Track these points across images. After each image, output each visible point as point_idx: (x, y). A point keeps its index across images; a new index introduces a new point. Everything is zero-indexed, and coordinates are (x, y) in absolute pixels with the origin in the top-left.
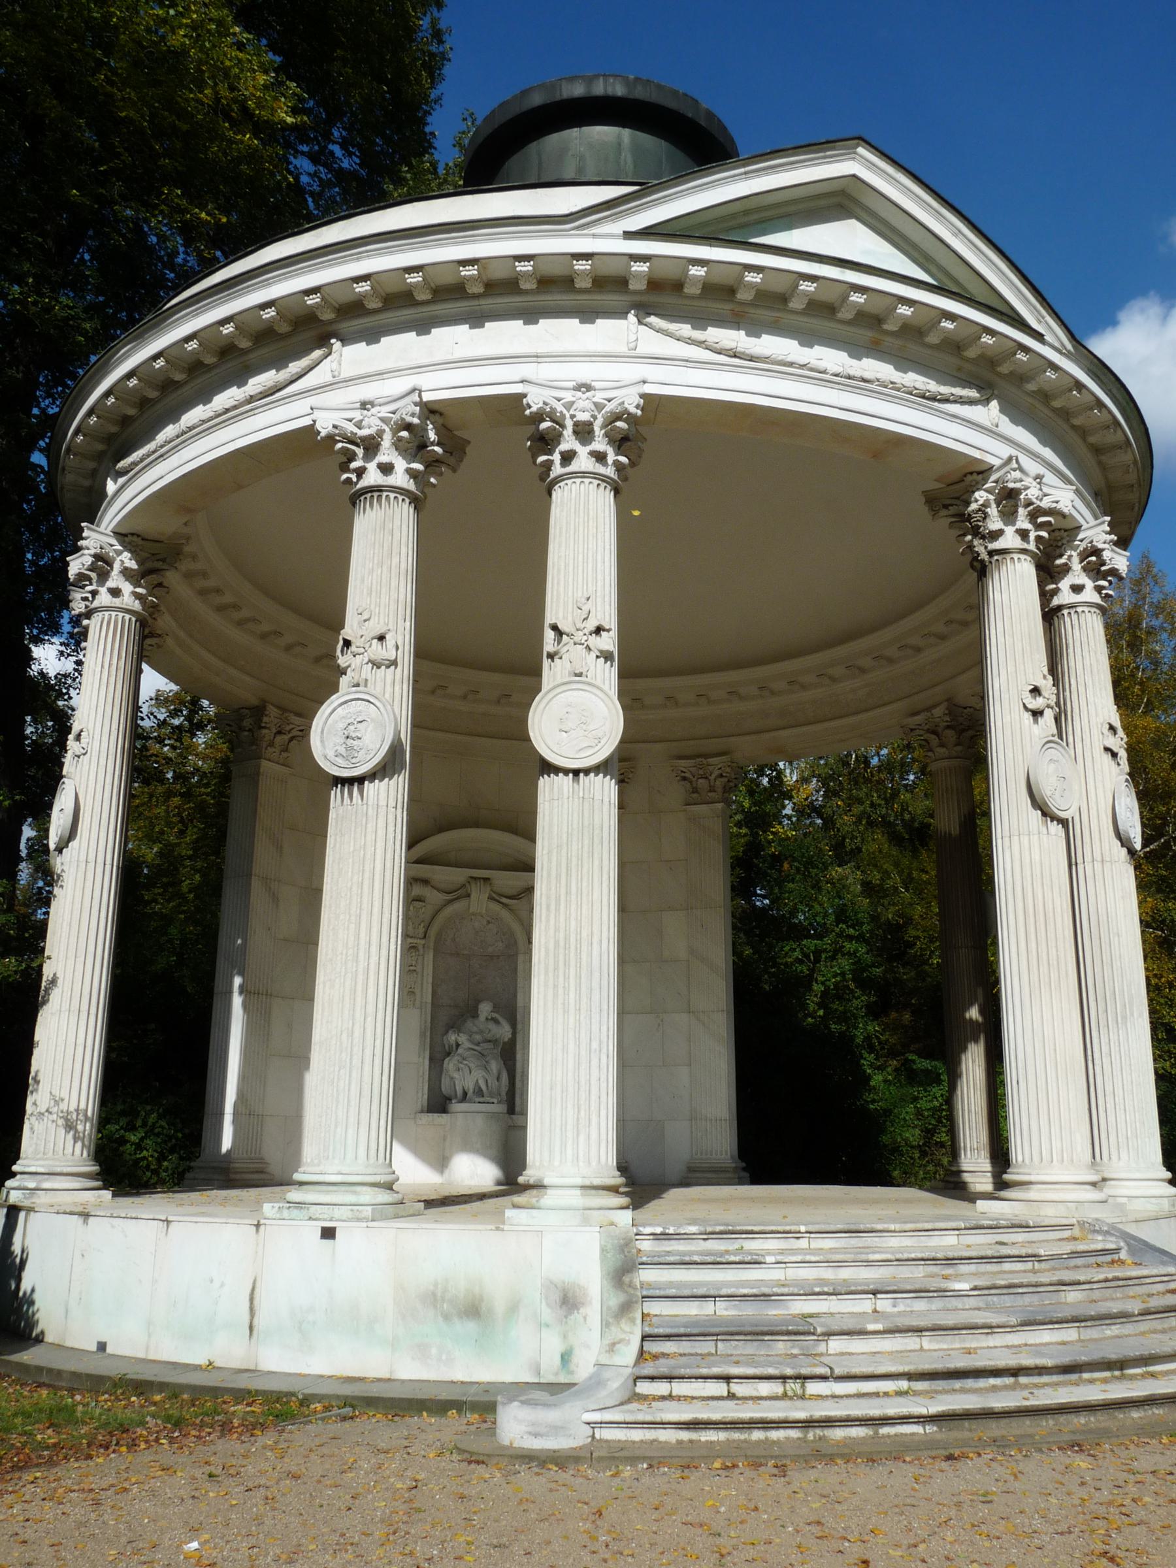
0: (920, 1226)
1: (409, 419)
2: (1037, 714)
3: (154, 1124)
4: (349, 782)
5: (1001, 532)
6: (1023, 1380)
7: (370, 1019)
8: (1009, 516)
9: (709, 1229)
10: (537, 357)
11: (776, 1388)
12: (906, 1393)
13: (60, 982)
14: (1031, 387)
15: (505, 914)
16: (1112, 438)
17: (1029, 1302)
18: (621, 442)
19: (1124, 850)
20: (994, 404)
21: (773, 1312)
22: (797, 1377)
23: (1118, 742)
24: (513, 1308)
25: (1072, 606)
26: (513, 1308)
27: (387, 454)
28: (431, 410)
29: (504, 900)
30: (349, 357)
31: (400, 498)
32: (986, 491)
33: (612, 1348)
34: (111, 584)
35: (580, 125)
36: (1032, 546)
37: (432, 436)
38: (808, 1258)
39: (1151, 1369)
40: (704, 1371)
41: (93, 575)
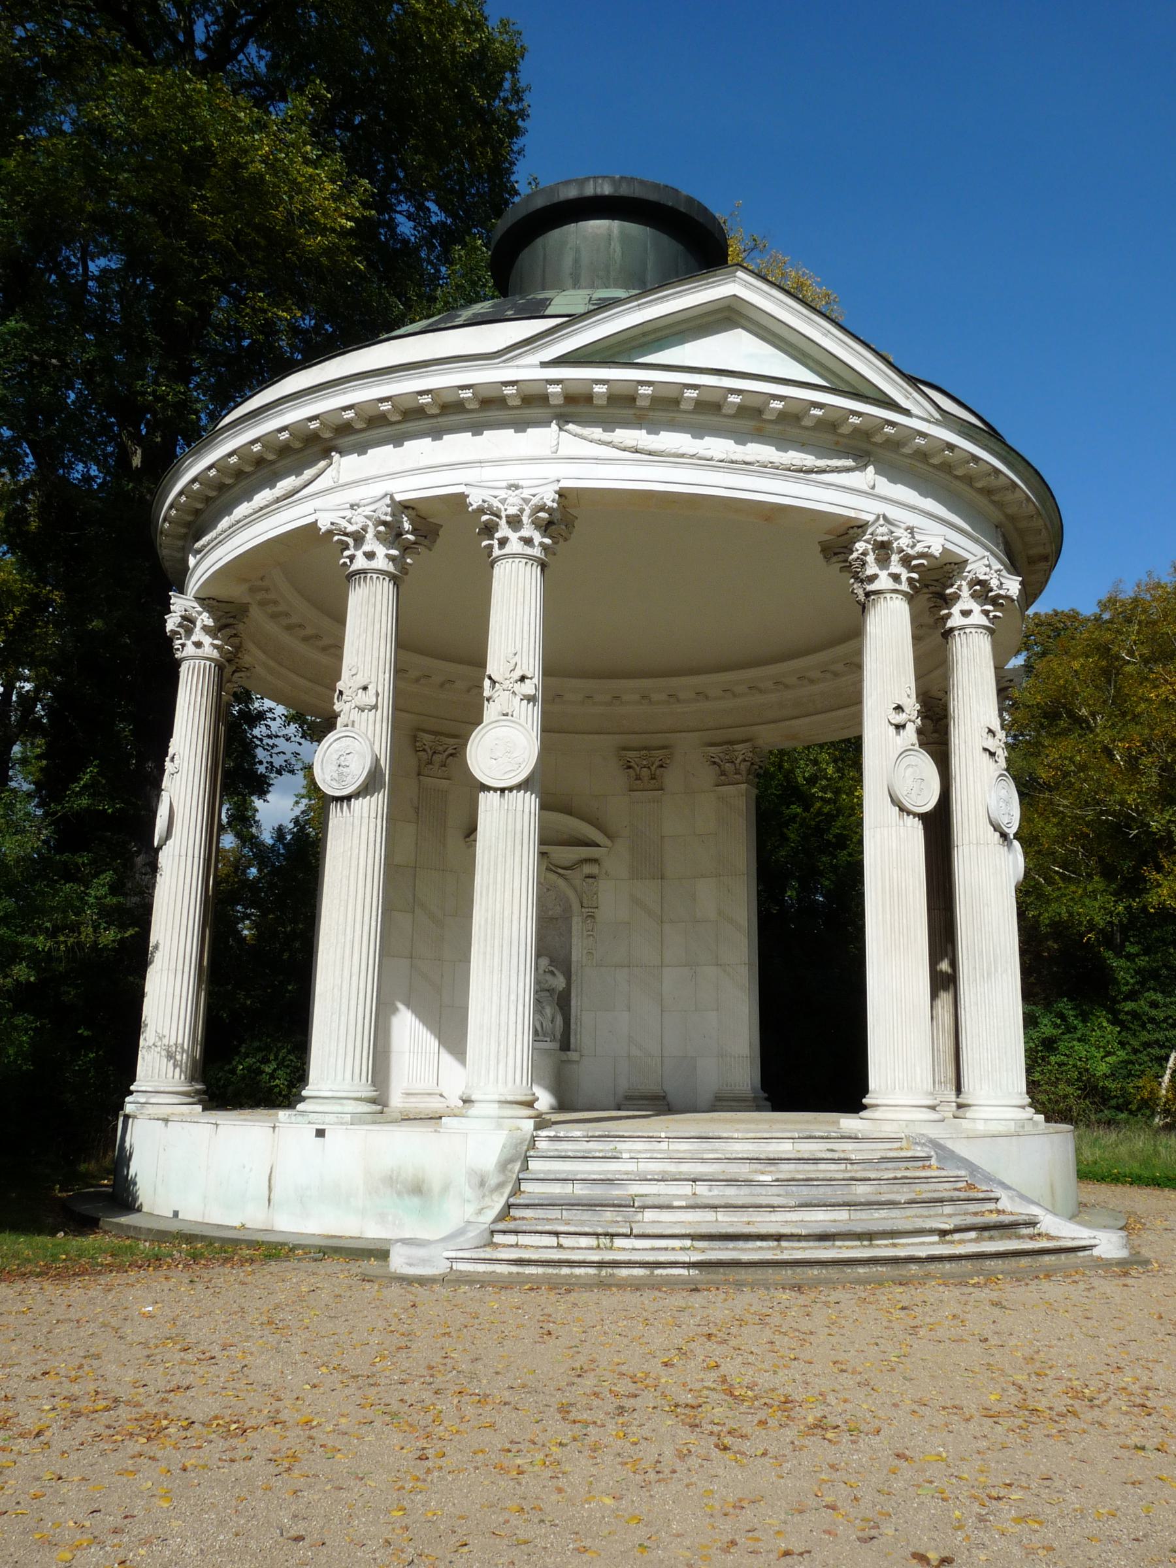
0: (759, 1135)
1: (383, 518)
2: (899, 727)
3: (284, 1058)
4: (340, 799)
5: (875, 577)
6: (784, 1244)
7: (355, 978)
8: (883, 562)
9: (590, 1134)
10: (480, 463)
11: (592, 1242)
12: (689, 1249)
13: (161, 947)
14: (906, 450)
15: (561, 882)
16: (1002, 481)
17: (806, 1193)
18: (546, 527)
19: (997, 834)
20: (871, 469)
21: (616, 1192)
22: (606, 1235)
23: (997, 745)
24: (446, 1188)
25: (961, 628)
26: (446, 1188)
27: (371, 543)
28: (405, 507)
29: (560, 871)
30: (345, 466)
31: (381, 577)
32: (865, 541)
33: (480, 1211)
34: (194, 638)
35: (577, 221)
36: (904, 587)
37: (407, 526)
38: (655, 1155)
39: (896, 1241)
40: (539, 1228)
41: (181, 631)
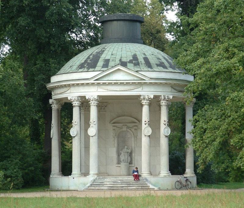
15: (130, 131)
